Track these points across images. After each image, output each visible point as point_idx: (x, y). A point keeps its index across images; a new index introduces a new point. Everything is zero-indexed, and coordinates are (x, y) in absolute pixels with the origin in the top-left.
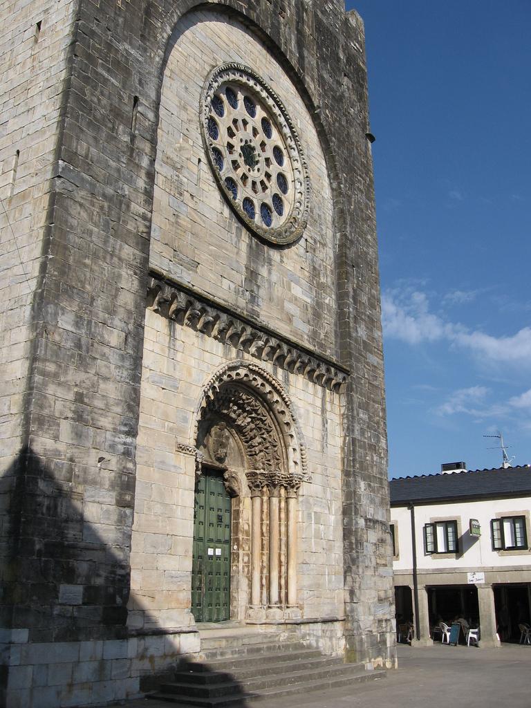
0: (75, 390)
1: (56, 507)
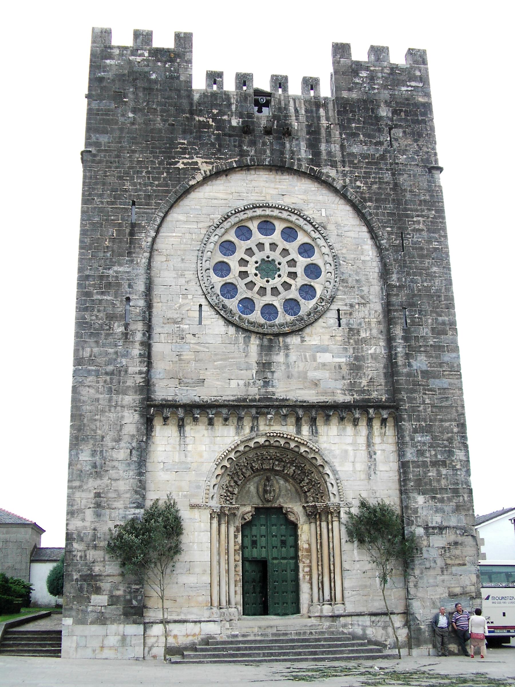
0: (94, 491)
1: (86, 556)
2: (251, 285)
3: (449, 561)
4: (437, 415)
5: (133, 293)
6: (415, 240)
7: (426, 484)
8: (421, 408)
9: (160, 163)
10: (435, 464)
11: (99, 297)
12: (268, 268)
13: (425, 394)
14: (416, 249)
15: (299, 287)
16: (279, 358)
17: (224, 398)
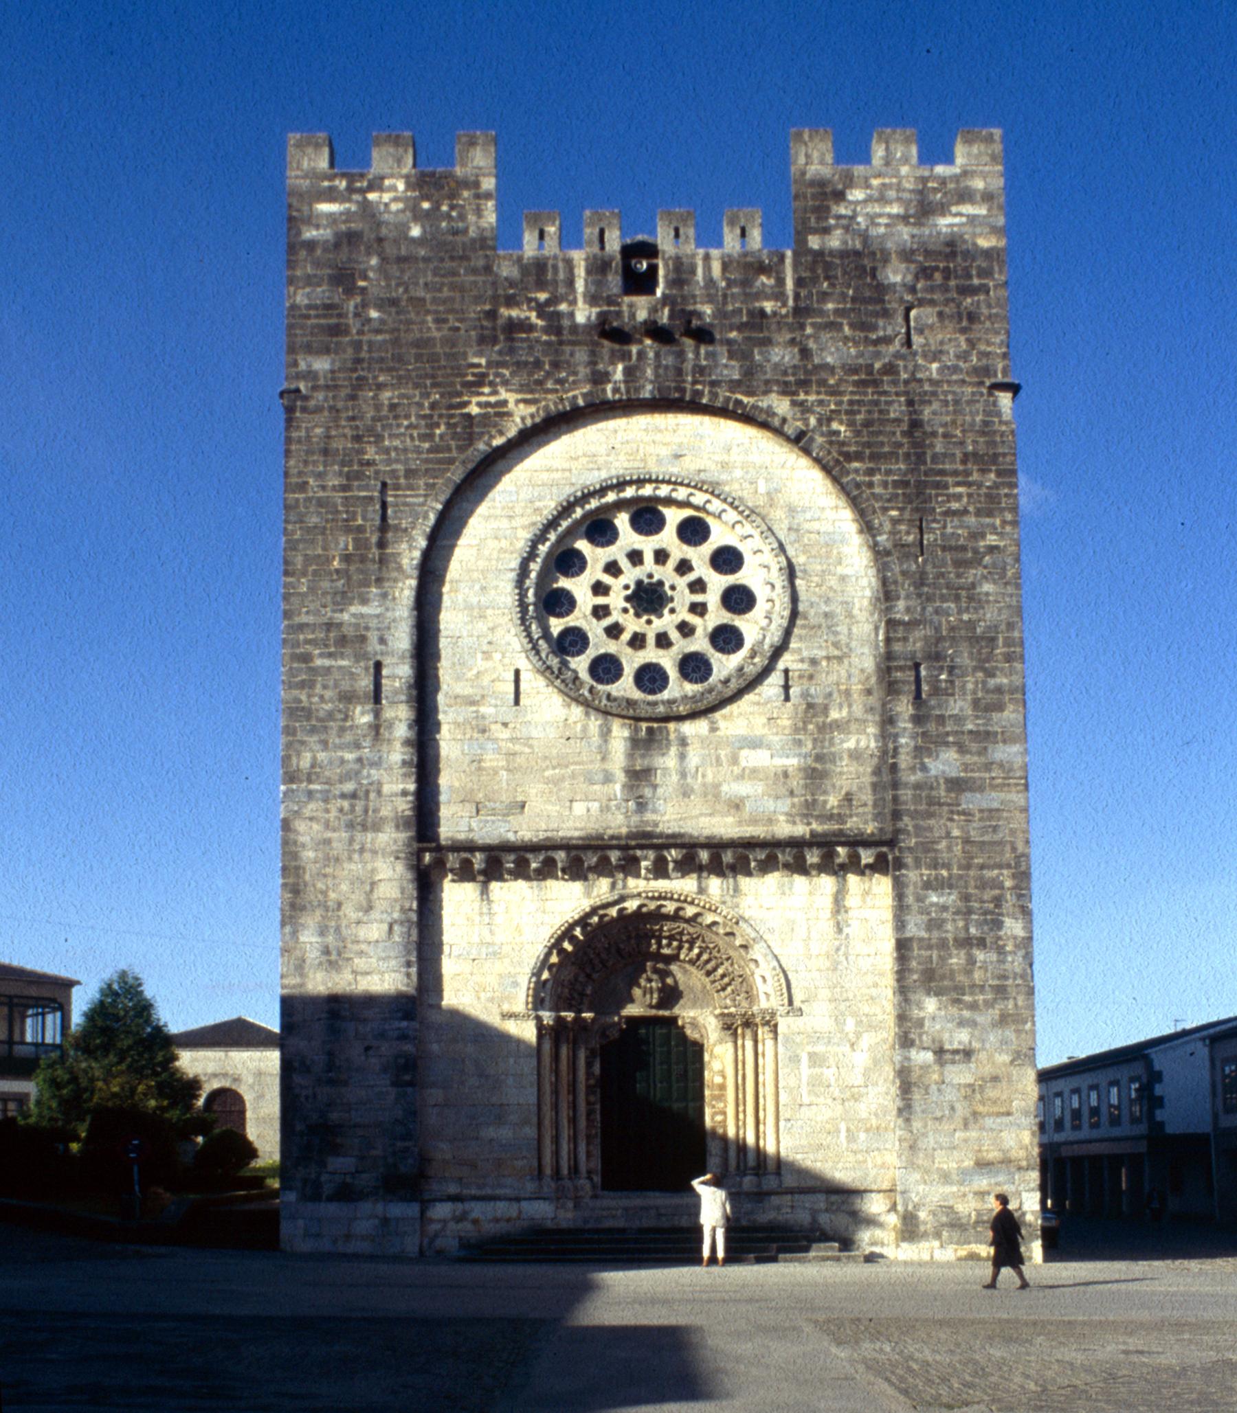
2: (614, 631)
3: (981, 1109)
4: (972, 858)
5: (387, 653)
6: (949, 530)
7: (943, 977)
8: (943, 845)
9: (433, 406)
10: (966, 942)
11: (327, 662)
12: (648, 598)
13: (951, 820)
14: (951, 549)
15: (710, 629)
16: (668, 761)
17: (561, 834)
